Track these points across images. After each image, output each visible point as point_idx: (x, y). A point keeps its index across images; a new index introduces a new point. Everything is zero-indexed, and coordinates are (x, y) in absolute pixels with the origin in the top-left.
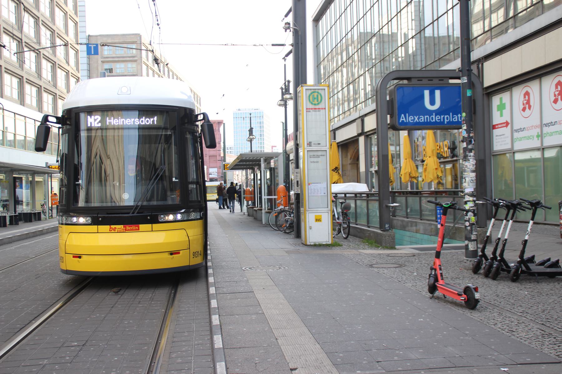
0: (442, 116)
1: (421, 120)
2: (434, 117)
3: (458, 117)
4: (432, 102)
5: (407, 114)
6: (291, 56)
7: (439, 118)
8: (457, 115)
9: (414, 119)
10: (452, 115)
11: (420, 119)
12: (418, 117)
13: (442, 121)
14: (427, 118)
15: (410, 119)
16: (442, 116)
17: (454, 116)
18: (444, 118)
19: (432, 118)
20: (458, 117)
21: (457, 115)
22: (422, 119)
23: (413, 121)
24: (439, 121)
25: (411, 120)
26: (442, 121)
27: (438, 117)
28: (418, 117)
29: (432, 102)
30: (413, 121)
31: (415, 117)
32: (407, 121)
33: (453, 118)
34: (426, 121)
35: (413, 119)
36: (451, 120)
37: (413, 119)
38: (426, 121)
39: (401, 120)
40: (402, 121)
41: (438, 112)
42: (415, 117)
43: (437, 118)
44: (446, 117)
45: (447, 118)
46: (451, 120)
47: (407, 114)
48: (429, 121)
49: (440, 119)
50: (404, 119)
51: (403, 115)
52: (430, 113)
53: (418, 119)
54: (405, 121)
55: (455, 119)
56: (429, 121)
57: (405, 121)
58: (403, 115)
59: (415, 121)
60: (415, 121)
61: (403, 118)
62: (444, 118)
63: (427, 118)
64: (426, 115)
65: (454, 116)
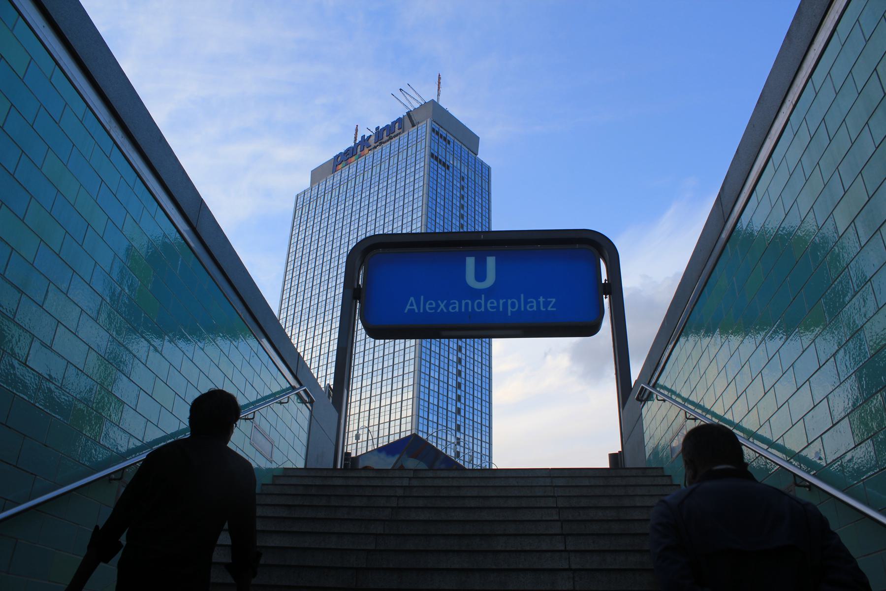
1: (454, 308)
2: (483, 302)
3: (538, 303)
4: (481, 275)
5: (422, 297)
6: (165, 434)
7: (495, 305)
8: (537, 299)
9: (438, 306)
11: (451, 307)
12: (445, 302)
13: (501, 309)
14: (467, 304)
15: (427, 306)
16: (501, 302)
17: (529, 300)
18: (505, 305)
19: (479, 306)
20: (538, 303)
21: (537, 299)
22: (456, 307)
23: (433, 311)
24: (495, 310)
25: (430, 309)
26: (501, 309)
27: (492, 303)
28: (445, 302)
29: (481, 275)
30: (433, 311)
31: (439, 302)
32: (422, 311)
33: (526, 303)
34: (463, 310)
35: (434, 305)
36: (523, 309)
37: (434, 305)
38: (463, 310)
39: (408, 307)
40: (409, 309)
41: (489, 293)
42: (439, 302)
43: (489, 305)
45: (513, 305)
46: (523, 309)
47: (422, 297)
48: (470, 310)
50: (415, 307)
51: (412, 299)
52: (475, 294)
53: (447, 306)
55: (532, 307)
56: (470, 310)
58: (412, 299)
59: (439, 311)
60: (439, 311)
61: (412, 305)
62: (505, 304)
63: (467, 304)
64: (465, 300)
65: (529, 300)
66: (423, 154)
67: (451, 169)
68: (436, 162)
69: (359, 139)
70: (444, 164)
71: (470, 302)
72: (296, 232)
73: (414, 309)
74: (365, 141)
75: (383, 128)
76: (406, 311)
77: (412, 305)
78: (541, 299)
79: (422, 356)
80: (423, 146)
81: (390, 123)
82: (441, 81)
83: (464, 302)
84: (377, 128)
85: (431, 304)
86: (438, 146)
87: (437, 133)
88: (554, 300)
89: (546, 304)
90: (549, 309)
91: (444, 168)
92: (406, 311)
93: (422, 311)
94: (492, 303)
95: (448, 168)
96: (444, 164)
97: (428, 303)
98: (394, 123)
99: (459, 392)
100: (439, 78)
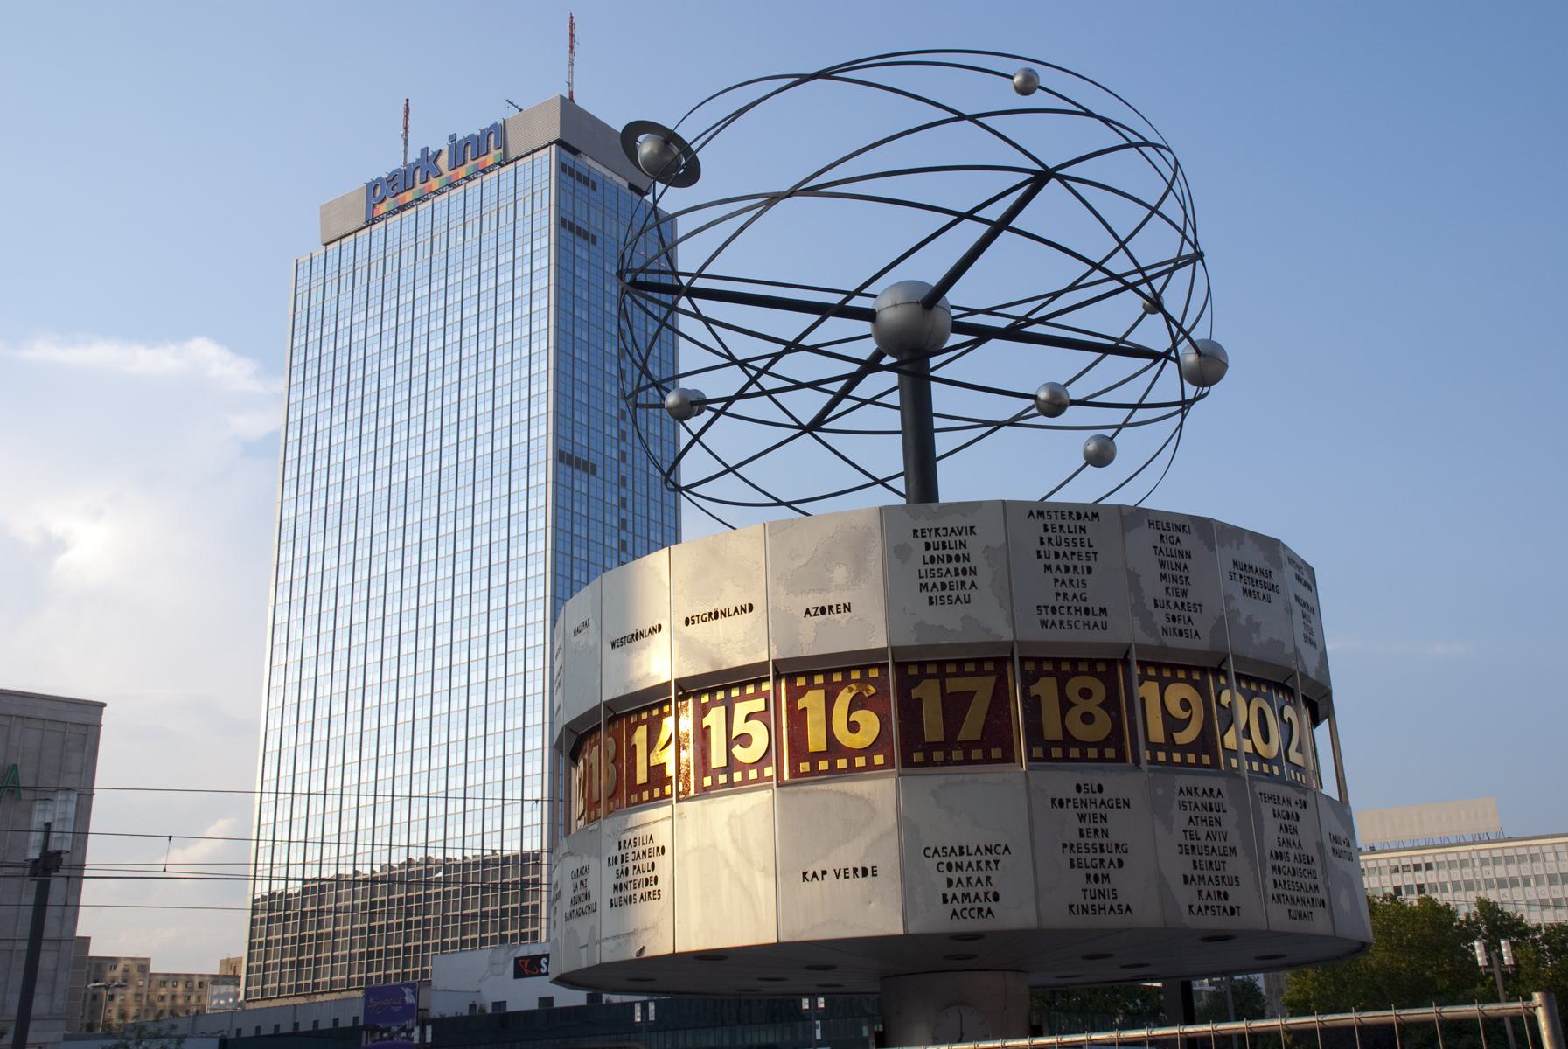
66: (546, 220)
67: (599, 188)
68: (570, 235)
69: (414, 155)
70: (586, 235)
72: (300, 341)
74: (428, 161)
75: (465, 139)
79: (558, 568)
80: (546, 205)
81: (478, 133)
82: (575, 32)
84: (453, 138)
86: (573, 200)
87: (571, 172)
91: (585, 244)
95: (594, 240)
96: (586, 235)
98: (487, 133)
99: (623, 535)
100: (572, 25)
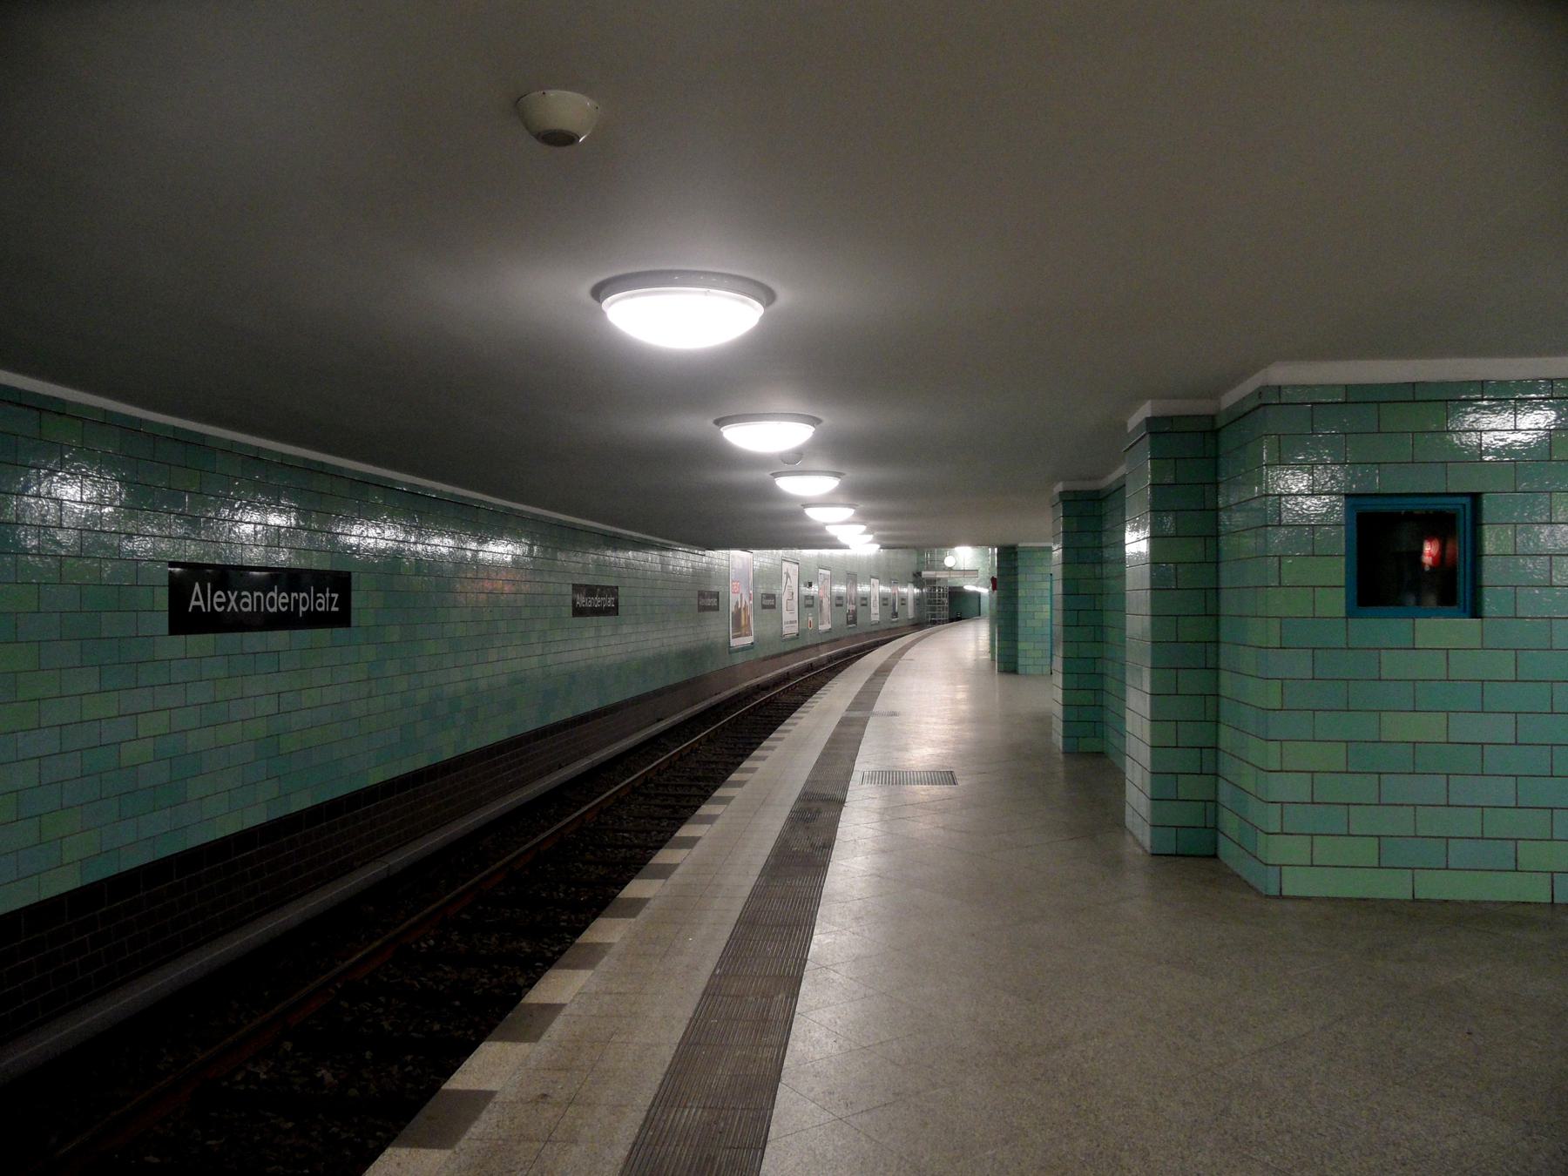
0: (293, 595)
2: (275, 596)
5: (209, 585)
7: (287, 601)
8: (324, 594)
9: (228, 600)
10: (315, 594)
12: (236, 593)
14: (259, 597)
17: (318, 595)
18: (296, 602)
21: (324, 594)
25: (219, 605)
27: (284, 598)
32: (209, 610)
33: (316, 599)
37: (224, 600)
39: (193, 603)
40: (193, 606)
44: (302, 595)
47: (209, 585)
48: (262, 610)
49: (289, 604)
50: (201, 603)
53: (238, 601)
54: (204, 610)
56: (262, 610)
57: (204, 610)
61: (197, 599)
71: (262, 595)
73: (200, 606)
76: (190, 610)
77: (197, 599)
78: (328, 595)
83: (256, 594)
85: (220, 597)
88: (336, 596)
89: (332, 599)
90: (334, 609)
92: (190, 610)
93: (209, 610)
94: (284, 598)
97: (216, 595)
